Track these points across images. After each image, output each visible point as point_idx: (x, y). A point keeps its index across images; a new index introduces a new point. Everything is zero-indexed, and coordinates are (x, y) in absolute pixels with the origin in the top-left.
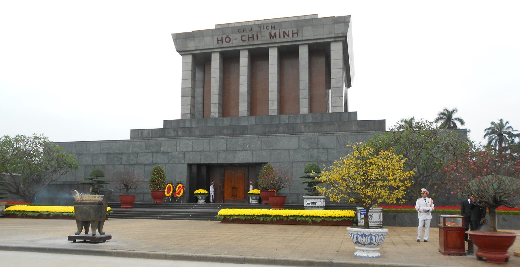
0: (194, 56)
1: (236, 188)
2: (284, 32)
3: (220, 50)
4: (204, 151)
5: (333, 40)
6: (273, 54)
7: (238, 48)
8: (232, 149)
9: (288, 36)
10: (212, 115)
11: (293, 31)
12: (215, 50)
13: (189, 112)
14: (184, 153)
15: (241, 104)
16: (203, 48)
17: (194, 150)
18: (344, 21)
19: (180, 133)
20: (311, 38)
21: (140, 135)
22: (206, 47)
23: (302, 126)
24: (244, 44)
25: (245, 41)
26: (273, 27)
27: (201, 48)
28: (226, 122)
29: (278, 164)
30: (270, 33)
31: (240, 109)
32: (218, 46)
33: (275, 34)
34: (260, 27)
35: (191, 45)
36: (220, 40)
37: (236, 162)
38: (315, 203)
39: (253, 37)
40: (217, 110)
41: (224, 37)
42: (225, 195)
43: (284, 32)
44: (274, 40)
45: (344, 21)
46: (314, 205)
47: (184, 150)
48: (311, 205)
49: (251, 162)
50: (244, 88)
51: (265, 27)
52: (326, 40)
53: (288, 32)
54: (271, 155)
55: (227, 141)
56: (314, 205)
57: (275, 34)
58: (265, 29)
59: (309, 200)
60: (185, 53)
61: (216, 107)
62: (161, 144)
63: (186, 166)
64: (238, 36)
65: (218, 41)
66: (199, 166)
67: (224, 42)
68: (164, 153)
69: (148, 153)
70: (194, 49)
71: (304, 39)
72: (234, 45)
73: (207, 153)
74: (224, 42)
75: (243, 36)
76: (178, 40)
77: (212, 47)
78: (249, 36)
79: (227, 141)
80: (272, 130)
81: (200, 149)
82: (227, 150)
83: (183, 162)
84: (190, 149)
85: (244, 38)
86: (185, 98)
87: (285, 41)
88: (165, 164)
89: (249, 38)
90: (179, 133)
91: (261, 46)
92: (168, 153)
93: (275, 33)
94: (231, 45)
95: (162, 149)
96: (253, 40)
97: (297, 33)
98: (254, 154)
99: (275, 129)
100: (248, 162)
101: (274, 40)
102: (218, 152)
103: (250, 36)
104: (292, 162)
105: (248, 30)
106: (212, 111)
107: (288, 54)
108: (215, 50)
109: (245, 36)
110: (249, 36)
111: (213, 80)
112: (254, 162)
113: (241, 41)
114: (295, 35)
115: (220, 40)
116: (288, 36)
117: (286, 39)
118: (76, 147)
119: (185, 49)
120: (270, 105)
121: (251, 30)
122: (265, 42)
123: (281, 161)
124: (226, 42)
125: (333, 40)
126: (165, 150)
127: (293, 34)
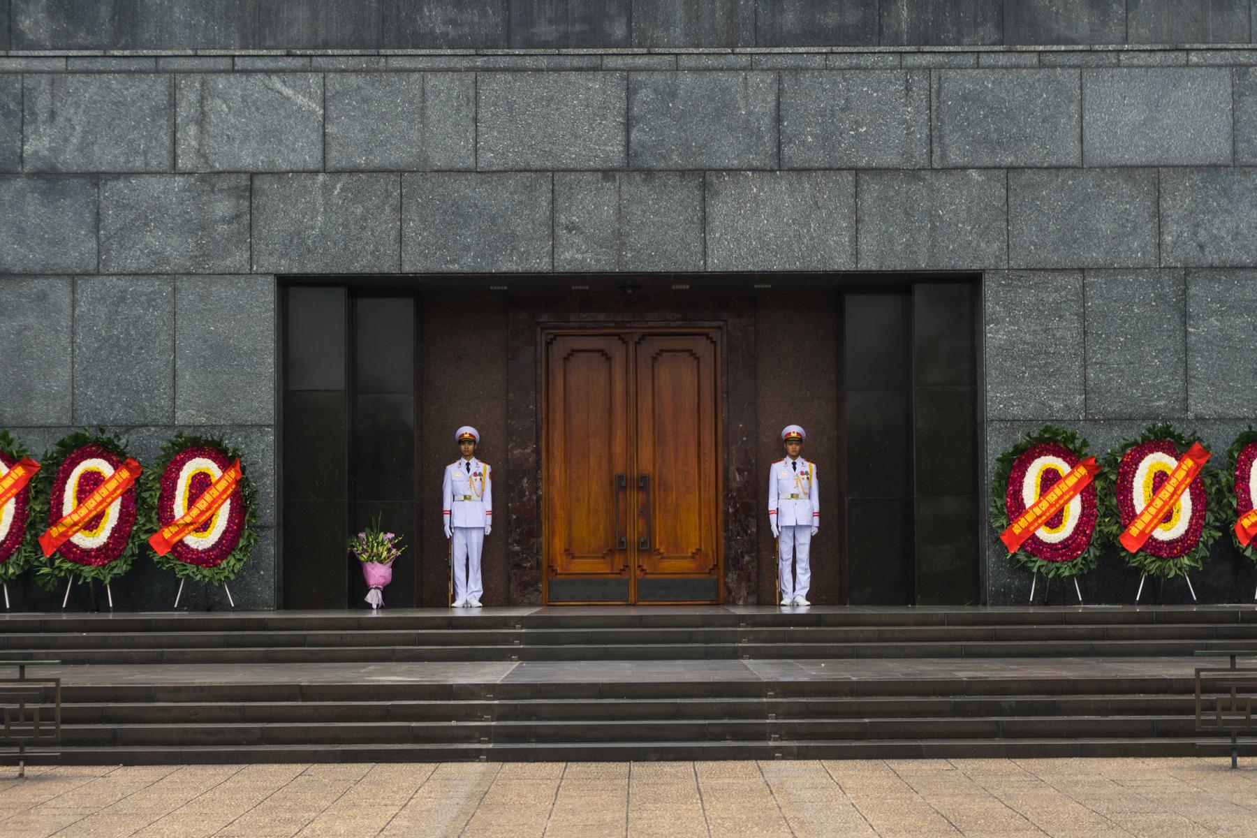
1: (643, 483)
4: (422, 169)
8: (676, 160)
14: (249, 184)
17: (336, 158)
29: (1074, 282)
37: (717, 262)
42: (559, 544)
47: (247, 160)
49: (842, 262)
54: (1007, 214)
55: (630, 92)
62: (24, 98)
63: (267, 294)
66: (359, 288)
68: (50, 178)
73: (464, 189)
79: (630, 92)
80: (830, 19)
81: (397, 156)
82: (633, 167)
83: (237, 259)
84: (301, 151)
88: (73, 276)
90: (25, 23)
92: (96, 178)
95: (37, 145)
98: (868, 200)
99: (852, 17)
100: (814, 263)
104: (1188, 273)
112: (869, 263)
123: (1096, 256)
126: (70, 159)
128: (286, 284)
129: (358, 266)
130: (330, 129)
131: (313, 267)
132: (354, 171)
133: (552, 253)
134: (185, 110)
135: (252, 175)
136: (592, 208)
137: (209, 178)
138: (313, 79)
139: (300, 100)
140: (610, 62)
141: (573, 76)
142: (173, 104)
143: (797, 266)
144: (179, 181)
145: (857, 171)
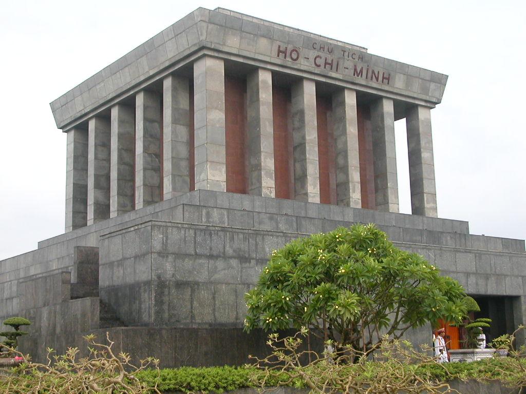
2: (373, 72)
5: (423, 103)
9: (377, 79)
10: (265, 191)
16: (252, 56)
18: (440, 80)
22: (257, 57)
23: (449, 238)
24: (317, 71)
25: (319, 66)
28: (288, 206)
32: (278, 61)
33: (361, 71)
34: (344, 51)
35: (233, 44)
39: (331, 65)
41: (290, 47)
45: (438, 81)
49: (505, 294)
55: (476, 257)
58: (350, 58)
60: (216, 54)
61: (271, 178)
64: (312, 54)
65: (279, 51)
70: (235, 51)
71: (395, 91)
72: (302, 68)
74: (288, 59)
76: (211, 26)
77: (268, 59)
85: (318, 61)
89: (326, 63)
91: (338, 83)
93: (362, 68)
96: (331, 69)
97: (388, 79)
102: (468, 274)
103: (330, 62)
105: (326, 49)
106: (264, 184)
113: (314, 65)
116: (377, 79)
118: (232, 239)
119: (221, 48)
122: (346, 79)
125: (423, 103)
127: (383, 78)
130: (436, 262)
133: (468, 290)
136: (472, 280)
139: (431, 255)
141: (468, 254)
145: (504, 275)
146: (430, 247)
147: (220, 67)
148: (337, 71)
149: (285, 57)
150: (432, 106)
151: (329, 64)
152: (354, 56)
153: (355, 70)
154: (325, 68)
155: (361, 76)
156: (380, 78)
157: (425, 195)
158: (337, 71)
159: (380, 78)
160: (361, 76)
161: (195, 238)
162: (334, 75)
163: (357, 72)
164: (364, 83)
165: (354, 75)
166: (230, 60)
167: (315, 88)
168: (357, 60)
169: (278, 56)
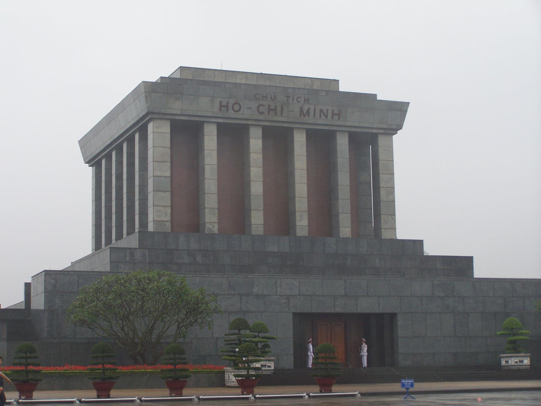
0: (171, 122)
2: (321, 111)
3: (221, 121)
5: (382, 131)
6: (300, 141)
7: (249, 122)
9: (326, 116)
10: (208, 226)
11: (333, 110)
12: (213, 120)
13: (168, 218)
14: (288, 297)
15: (253, 213)
19: (199, 259)
20: (357, 124)
21: (128, 259)
22: (199, 114)
24: (261, 117)
25: (262, 113)
26: (307, 101)
27: (191, 113)
30: (301, 108)
31: (253, 221)
33: (308, 111)
34: (288, 97)
36: (224, 106)
37: (359, 311)
38: (522, 361)
39: (275, 110)
40: (215, 219)
43: (321, 111)
44: (306, 119)
46: (521, 364)
48: (519, 364)
49: (377, 311)
50: (257, 188)
51: (295, 98)
52: (374, 131)
53: (327, 110)
55: (345, 283)
56: (521, 364)
57: (308, 111)
58: (295, 102)
59: (516, 358)
60: (161, 116)
63: (291, 315)
65: (221, 106)
66: (300, 314)
67: (231, 111)
68: (258, 296)
69: (234, 295)
70: (179, 112)
71: (348, 124)
74: (231, 111)
75: (261, 105)
77: (211, 114)
78: (269, 106)
83: (287, 309)
85: (261, 109)
86: (161, 194)
87: (321, 123)
89: (270, 110)
91: (284, 125)
93: (309, 109)
94: (241, 117)
95: (255, 290)
96: (276, 114)
97: (339, 115)
100: (374, 311)
101: (306, 119)
103: (272, 107)
106: (207, 220)
107: (322, 142)
108: (213, 120)
109: (264, 106)
110: (269, 106)
111: (207, 169)
113: (257, 113)
114: (336, 117)
115: (224, 106)
116: (326, 116)
117: (323, 120)
119: (163, 111)
120: (298, 218)
121: (274, 99)
124: (234, 110)
125: (382, 131)
127: (333, 114)
128: (294, 314)
129: (305, 311)
131: (298, 311)
132: (304, 295)
134: (278, 285)
135: (289, 296)
137: (282, 296)
138: (298, 280)
140: (343, 278)
142: (276, 284)
143: (370, 312)
144: (277, 297)
146: (295, 277)
147: (166, 128)
148: (282, 114)
149: (227, 110)
150: (391, 132)
151: (272, 110)
152: (299, 100)
153: (301, 111)
154: (269, 114)
155: (309, 116)
156: (330, 116)
157: (382, 216)
158: (282, 114)
159: (330, 116)
160: (309, 116)
161: (78, 281)
162: (279, 119)
163: (303, 114)
164: (310, 121)
165: (301, 116)
166: (175, 119)
167: (261, 132)
168: (302, 102)
169: (220, 110)
